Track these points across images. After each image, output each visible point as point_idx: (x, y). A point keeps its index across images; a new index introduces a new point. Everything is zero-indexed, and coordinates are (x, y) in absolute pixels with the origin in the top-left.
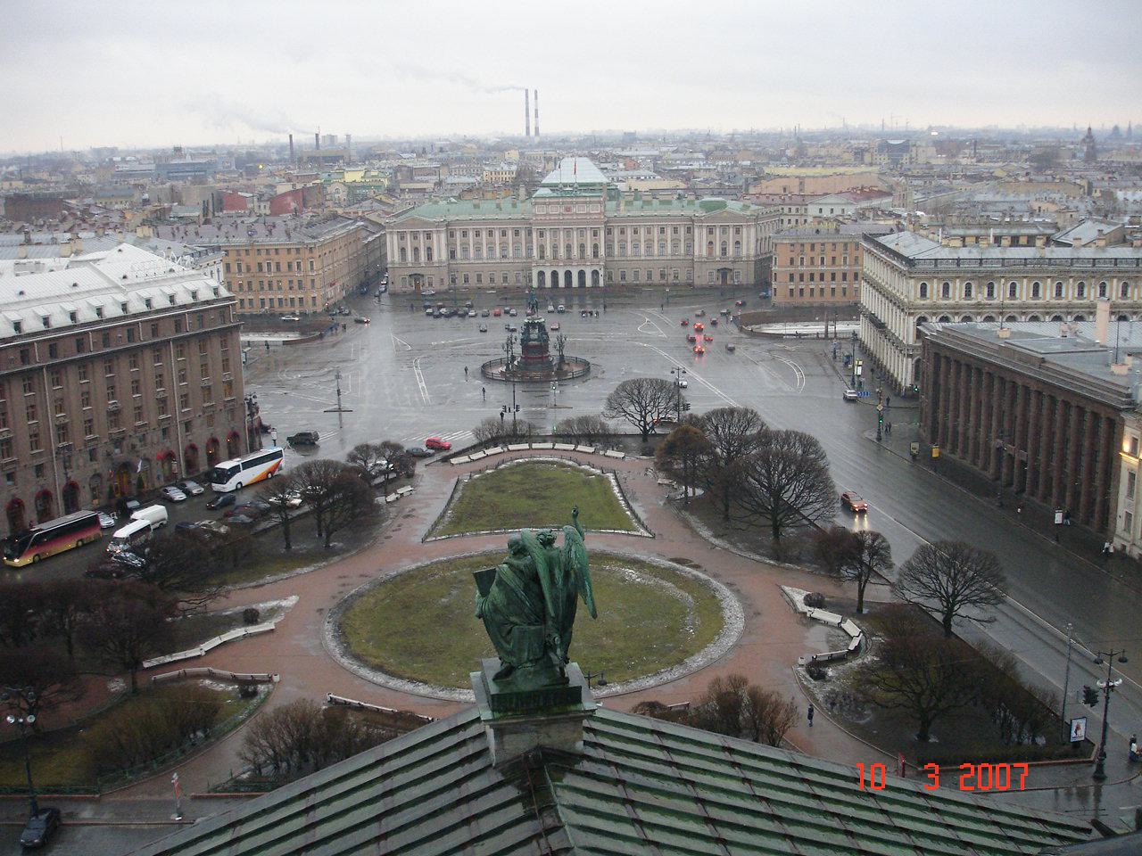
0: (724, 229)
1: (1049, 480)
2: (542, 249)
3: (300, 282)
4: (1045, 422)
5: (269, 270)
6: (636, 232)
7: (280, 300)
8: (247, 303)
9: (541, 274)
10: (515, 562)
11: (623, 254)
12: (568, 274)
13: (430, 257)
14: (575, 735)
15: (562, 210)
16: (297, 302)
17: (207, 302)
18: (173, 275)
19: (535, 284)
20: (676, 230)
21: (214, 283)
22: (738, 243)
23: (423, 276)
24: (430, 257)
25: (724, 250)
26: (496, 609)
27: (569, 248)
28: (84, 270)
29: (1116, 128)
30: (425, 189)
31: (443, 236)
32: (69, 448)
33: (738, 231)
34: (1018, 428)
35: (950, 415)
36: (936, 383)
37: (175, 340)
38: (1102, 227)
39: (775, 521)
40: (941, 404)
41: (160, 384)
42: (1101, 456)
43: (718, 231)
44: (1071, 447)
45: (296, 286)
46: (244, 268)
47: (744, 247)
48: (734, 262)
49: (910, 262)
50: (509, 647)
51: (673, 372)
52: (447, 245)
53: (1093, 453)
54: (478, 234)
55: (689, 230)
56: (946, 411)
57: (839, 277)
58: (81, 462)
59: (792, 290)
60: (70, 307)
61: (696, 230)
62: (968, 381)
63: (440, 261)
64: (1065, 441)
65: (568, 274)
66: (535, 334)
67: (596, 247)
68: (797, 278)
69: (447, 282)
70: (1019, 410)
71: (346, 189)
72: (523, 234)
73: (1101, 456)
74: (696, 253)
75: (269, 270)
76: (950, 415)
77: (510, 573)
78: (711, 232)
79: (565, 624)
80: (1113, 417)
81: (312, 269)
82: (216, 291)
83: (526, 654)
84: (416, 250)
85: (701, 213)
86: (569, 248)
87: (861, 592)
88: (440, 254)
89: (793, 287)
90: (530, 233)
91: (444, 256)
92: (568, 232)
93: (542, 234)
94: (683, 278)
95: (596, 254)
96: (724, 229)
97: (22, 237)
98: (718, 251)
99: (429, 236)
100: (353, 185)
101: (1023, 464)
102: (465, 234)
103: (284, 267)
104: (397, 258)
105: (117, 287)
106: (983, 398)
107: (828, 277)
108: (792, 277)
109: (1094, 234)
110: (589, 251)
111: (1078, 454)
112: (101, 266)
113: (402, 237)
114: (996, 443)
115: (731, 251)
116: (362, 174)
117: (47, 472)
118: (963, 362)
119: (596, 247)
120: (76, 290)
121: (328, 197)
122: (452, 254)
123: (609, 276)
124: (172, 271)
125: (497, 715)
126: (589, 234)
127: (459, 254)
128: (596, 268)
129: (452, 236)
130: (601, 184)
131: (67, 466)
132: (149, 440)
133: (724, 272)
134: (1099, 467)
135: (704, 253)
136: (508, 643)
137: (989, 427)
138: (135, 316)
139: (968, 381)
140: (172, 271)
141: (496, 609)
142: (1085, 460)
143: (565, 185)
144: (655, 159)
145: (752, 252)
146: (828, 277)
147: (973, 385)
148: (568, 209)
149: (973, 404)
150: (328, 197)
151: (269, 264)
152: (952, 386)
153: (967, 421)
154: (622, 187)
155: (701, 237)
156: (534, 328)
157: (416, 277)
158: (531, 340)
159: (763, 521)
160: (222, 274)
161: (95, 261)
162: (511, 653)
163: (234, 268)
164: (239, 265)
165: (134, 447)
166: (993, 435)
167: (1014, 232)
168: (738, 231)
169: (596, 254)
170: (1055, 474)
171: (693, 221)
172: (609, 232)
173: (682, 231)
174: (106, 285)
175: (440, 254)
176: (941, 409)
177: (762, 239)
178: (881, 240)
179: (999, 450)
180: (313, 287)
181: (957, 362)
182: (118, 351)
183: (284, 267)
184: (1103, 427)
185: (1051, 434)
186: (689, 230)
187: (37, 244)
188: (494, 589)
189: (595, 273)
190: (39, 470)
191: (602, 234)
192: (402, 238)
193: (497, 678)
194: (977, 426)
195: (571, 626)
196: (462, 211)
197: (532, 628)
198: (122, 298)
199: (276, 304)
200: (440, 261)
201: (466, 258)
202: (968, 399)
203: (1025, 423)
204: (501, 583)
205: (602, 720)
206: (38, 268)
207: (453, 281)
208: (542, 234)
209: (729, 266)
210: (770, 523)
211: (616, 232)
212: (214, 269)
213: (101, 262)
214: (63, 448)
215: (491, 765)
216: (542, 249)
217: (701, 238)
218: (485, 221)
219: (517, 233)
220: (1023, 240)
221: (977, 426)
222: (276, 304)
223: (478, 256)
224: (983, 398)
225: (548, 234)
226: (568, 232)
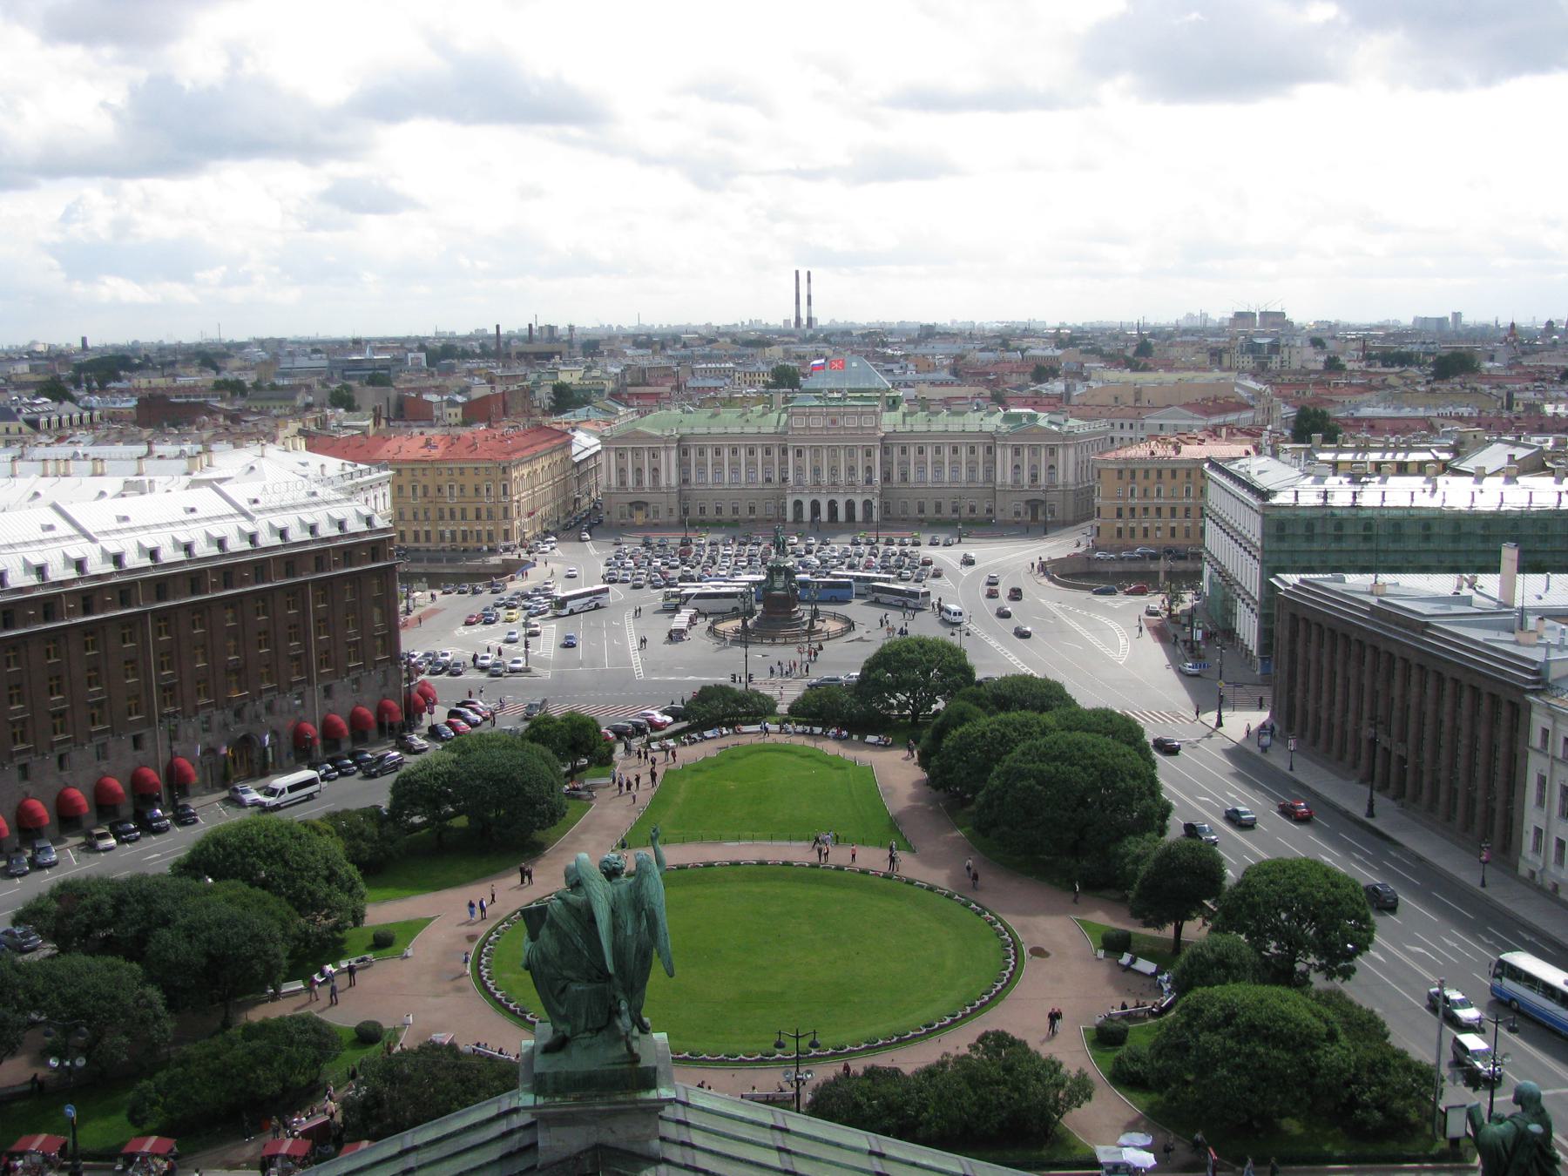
0: (1034, 450)
1: (1435, 784)
2: (799, 470)
3: (489, 512)
4: (1429, 708)
5: (451, 495)
6: (921, 451)
7: (464, 532)
8: (422, 536)
9: (798, 504)
10: (571, 897)
14: (648, 1131)
15: (827, 422)
16: (485, 537)
18: (315, 499)
19: (790, 516)
20: (972, 450)
21: (366, 511)
22: (1052, 467)
25: (1034, 477)
26: (545, 959)
28: (207, 491)
31: (674, 454)
32: (174, 715)
33: (1052, 451)
34: (1396, 714)
35: (1311, 696)
36: (1292, 652)
38: (1512, 451)
40: (1299, 680)
42: (1502, 752)
44: (1464, 741)
45: (484, 515)
46: (419, 492)
47: (1061, 472)
49: (1264, 495)
50: (562, 1011)
53: (1492, 750)
54: (718, 453)
56: (1306, 691)
57: (1180, 513)
58: (190, 732)
59: (1119, 531)
62: (1333, 652)
63: (669, 486)
64: (1456, 730)
66: (780, 582)
68: (1126, 513)
69: (676, 512)
70: (1396, 691)
72: (776, 452)
73: (1502, 752)
74: (999, 480)
75: (451, 495)
76: (1311, 696)
77: (564, 912)
78: (1017, 451)
79: (634, 983)
80: (1516, 699)
81: (505, 493)
82: (369, 520)
83: (582, 1022)
84: (639, 471)
85: (1004, 427)
87: (1178, 930)
89: (1120, 525)
90: (785, 452)
91: (674, 481)
92: (833, 450)
93: (799, 453)
94: (981, 513)
95: (869, 481)
96: (1034, 450)
101: (1402, 760)
102: (701, 453)
103: (470, 491)
105: (245, 514)
106: (1352, 672)
107: (1166, 512)
108: (1119, 515)
109: (1503, 461)
110: (860, 475)
111: (1473, 749)
113: (621, 455)
114: (1367, 732)
115: (1043, 479)
116: (580, 374)
117: (147, 743)
118: (1325, 626)
119: (869, 469)
121: (537, 403)
122: (686, 481)
123: (886, 508)
124: (314, 494)
125: (540, 1101)
129: (685, 453)
130: (878, 390)
131: (173, 736)
132: (277, 708)
133: (1034, 505)
134: (1500, 766)
135: (1009, 480)
136: (561, 1004)
137: (1359, 716)
138: (266, 549)
139: (1333, 652)
140: (314, 494)
141: (545, 959)
142: (1481, 757)
143: (831, 391)
144: (959, 358)
145: (1071, 479)
146: (1166, 512)
147: (1339, 656)
148: (834, 422)
149: (1339, 681)
150: (537, 403)
151: (451, 487)
152: (1312, 657)
153: (1332, 702)
155: (1004, 458)
156: (779, 574)
160: (388, 498)
161: (221, 480)
162: (564, 1019)
163: (408, 490)
164: (414, 488)
165: (257, 717)
166: (1365, 722)
168: (1052, 451)
170: (1443, 775)
172: (886, 450)
173: (981, 451)
175: (670, 476)
176: (1299, 686)
178: (1234, 467)
179: (1373, 742)
180: (506, 517)
181: (1320, 625)
183: (432, 491)
184: (1505, 713)
185: (1439, 723)
186: (989, 450)
187: (160, 457)
188: (544, 932)
189: (867, 504)
190: (137, 742)
191: (878, 453)
193: (548, 1049)
194: (1345, 711)
195: (643, 985)
196: (697, 421)
197: (594, 986)
198: (249, 528)
199: (459, 537)
200: (669, 486)
202: (1333, 673)
203: (1405, 709)
204: (553, 924)
205: (703, 1109)
207: (686, 512)
208: (799, 453)
211: (896, 451)
212: (380, 491)
214: (168, 715)
215: (534, 1167)
216: (799, 470)
217: (1004, 457)
218: (726, 436)
221: (1345, 711)
222: (459, 537)
224: (1352, 672)
225: (807, 455)
226: (833, 450)
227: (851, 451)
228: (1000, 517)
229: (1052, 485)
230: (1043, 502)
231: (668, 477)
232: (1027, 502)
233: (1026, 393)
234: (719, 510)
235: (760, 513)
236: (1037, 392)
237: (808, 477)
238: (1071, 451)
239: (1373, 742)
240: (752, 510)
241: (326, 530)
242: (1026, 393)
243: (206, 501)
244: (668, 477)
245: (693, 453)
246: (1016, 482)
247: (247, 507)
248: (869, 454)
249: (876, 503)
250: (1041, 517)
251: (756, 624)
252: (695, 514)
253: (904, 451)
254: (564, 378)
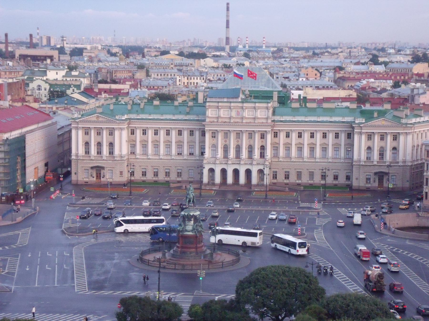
0: (383, 137)
9: (212, 171)
11: (288, 156)
12: (236, 172)
13: (111, 153)
15: (234, 114)
22: (394, 149)
23: (103, 168)
24: (111, 153)
27: (238, 149)
29: (32, 83)
30: (121, 90)
31: (125, 134)
33: (395, 138)
43: (377, 138)
48: (389, 166)
51: (307, 267)
52: (128, 141)
54: (156, 133)
55: (349, 136)
61: (356, 137)
65: (236, 172)
67: (263, 148)
71: (48, 87)
72: (197, 134)
74: (356, 157)
84: (99, 145)
86: (238, 149)
88: (122, 148)
90: (203, 134)
93: (214, 135)
94: (342, 180)
95: (262, 155)
98: (376, 156)
99: (111, 133)
100: (54, 83)
104: (81, 151)
113: (87, 132)
116: (63, 73)
119: (263, 148)
121: (29, 93)
122: (133, 153)
123: (275, 176)
126: (257, 137)
127: (138, 149)
128: (261, 167)
129: (133, 133)
133: (381, 176)
135: (363, 157)
145: (409, 158)
148: (238, 113)
150: (29, 93)
154: (295, 94)
155: (360, 143)
157: (99, 169)
158: (187, 231)
168: (395, 138)
169: (262, 155)
171: (353, 128)
173: (343, 137)
177: (418, 146)
189: (261, 172)
192: (87, 133)
201: (145, 153)
207: (132, 174)
208: (214, 135)
209: (386, 171)
219: (192, 133)
223: (157, 153)
225: (220, 136)
227: (251, 135)
228: (355, 184)
229: (395, 161)
230: (387, 174)
231: (121, 150)
232: (376, 174)
233: (384, 95)
234: (156, 174)
235: (185, 177)
236: (392, 95)
237: (220, 153)
238: (410, 137)
239: (77, 286)
240: (179, 174)
242: (384, 95)
244: (121, 150)
245: (139, 133)
246: (368, 158)
248: (263, 136)
249: (267, 171)
250: (385, 185)
251: (173, 256)
252: (138, 176)
253: (288, 136)
254: (52, 75)
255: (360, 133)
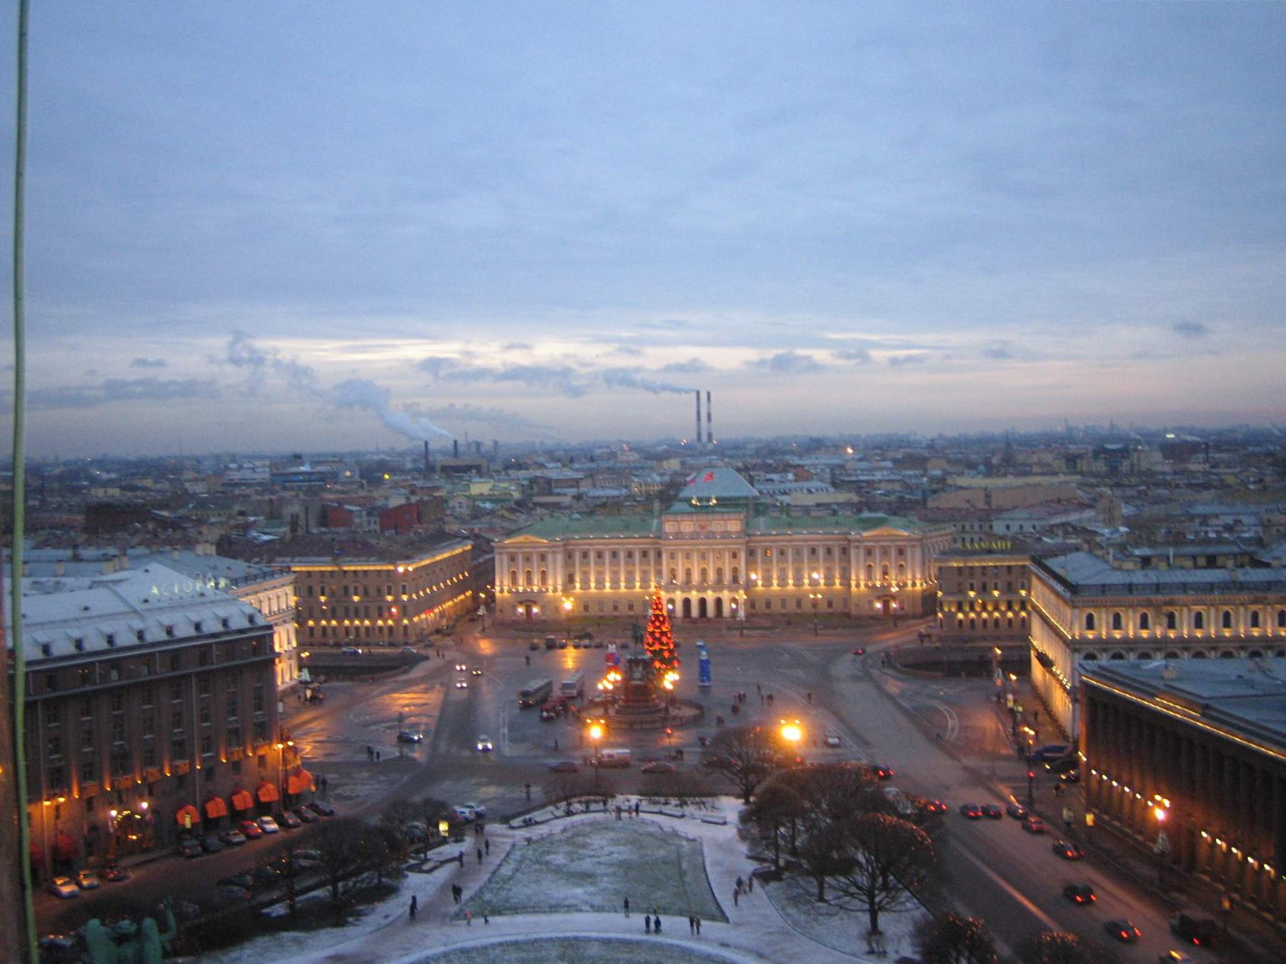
17: (241, 631)
18: (203, 599)
37: (198, 674)
39: (872, 903)
41: (178, 724)
49: (1073, 588)
60: (76, 634)
67: (735, 570)
90: (659, 555)
93: (672, 556)
97: (69, 553)
105: (135, 612)
112: (121, 589)
120: (88, 614)
130: (746, 498)
138: (153, 645)
150: (449, 512)
159: (856, 904)
161: (117, 582)
167: (1210, 550)
174: (123, 608)
182: (129, 685)
198: (137, 624)
206: (58, 587)
208: (672, 556)
210: (867, 906)
213: (123, 585)
220: (1202, 561)
241: (212, 626)
243: (102, 600)
247: (138, 608)
248: (734, 556)
255: (858, 547)
